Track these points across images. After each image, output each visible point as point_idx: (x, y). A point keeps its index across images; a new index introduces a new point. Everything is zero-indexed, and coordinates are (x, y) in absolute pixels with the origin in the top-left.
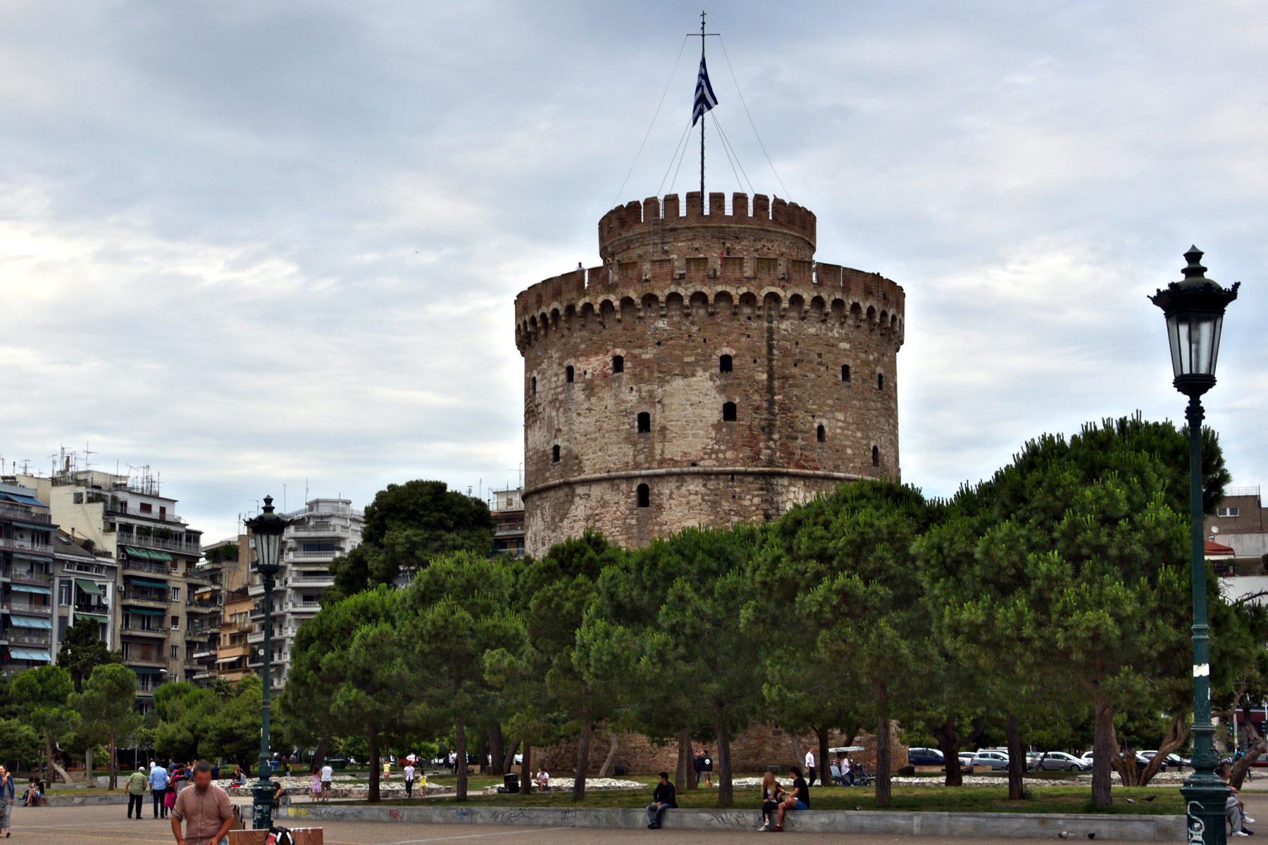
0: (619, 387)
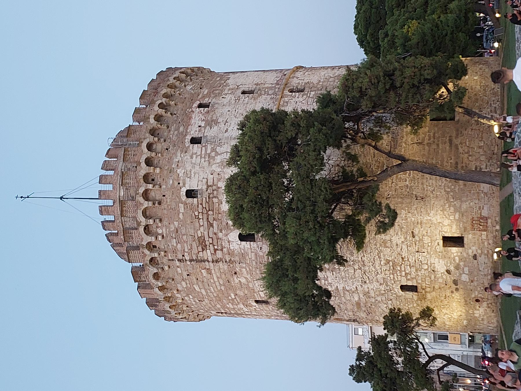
0: (219, 104)
